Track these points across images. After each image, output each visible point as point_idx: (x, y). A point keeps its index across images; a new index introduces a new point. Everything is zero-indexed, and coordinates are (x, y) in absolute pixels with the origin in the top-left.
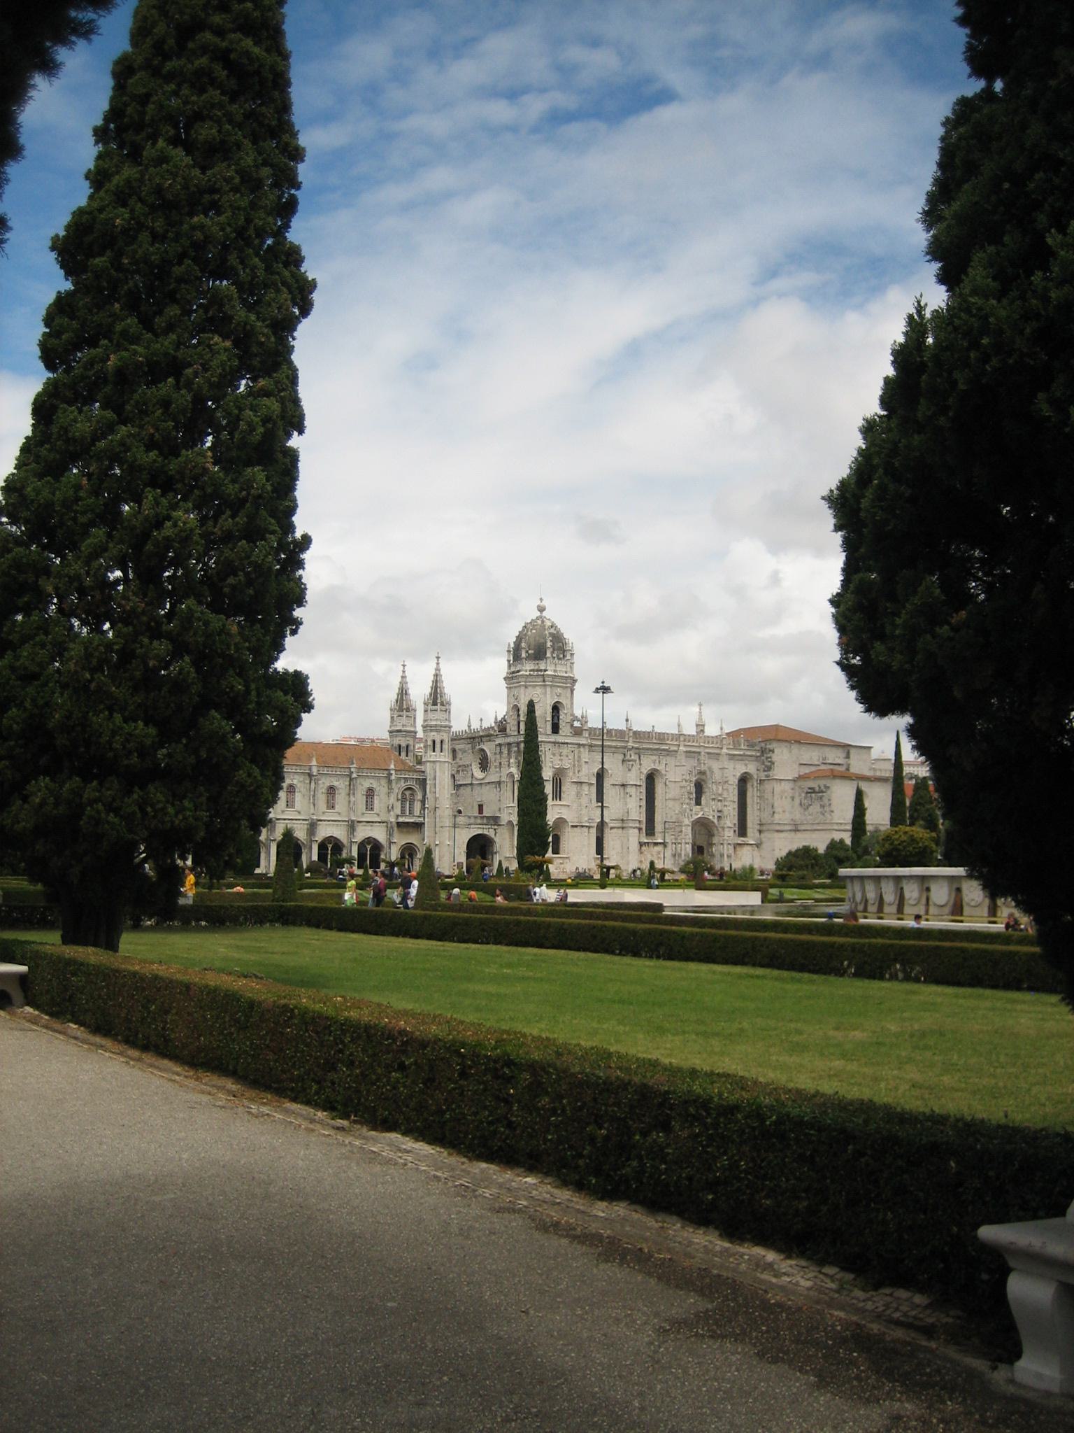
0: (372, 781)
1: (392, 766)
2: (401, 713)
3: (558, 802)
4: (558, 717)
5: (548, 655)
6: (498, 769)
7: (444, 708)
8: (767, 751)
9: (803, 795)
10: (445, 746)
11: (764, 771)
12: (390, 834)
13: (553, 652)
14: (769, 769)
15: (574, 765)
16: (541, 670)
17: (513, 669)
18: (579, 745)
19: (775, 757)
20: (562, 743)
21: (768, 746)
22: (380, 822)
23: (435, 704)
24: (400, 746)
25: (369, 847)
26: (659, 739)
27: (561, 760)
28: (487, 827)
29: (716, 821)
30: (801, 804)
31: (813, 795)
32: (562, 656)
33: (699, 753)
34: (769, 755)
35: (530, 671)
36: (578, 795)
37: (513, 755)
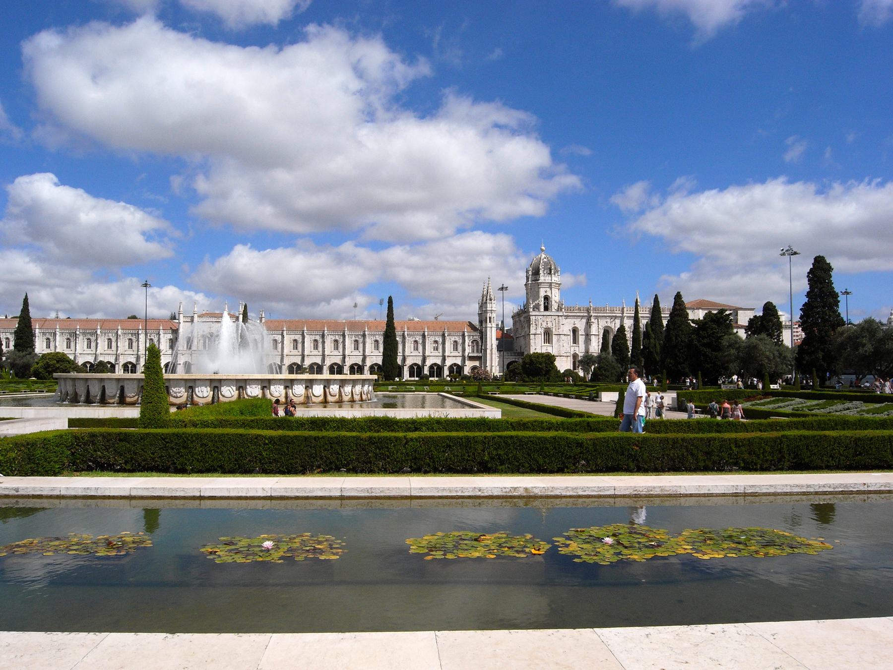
0: (456, 337)
3: (548, 344)
4: (548, 303)
5: (541, 272)
7: (490, 302)
10: (492, 320)
12: (464, 361)
13: (544, 271)
15: (556, 326)
18: (558, 316)
20: (548, 316)
25: (455, 368)
26: (611, 310)
27: (547, 324)
32: (548, 272)
36: (558, 340)
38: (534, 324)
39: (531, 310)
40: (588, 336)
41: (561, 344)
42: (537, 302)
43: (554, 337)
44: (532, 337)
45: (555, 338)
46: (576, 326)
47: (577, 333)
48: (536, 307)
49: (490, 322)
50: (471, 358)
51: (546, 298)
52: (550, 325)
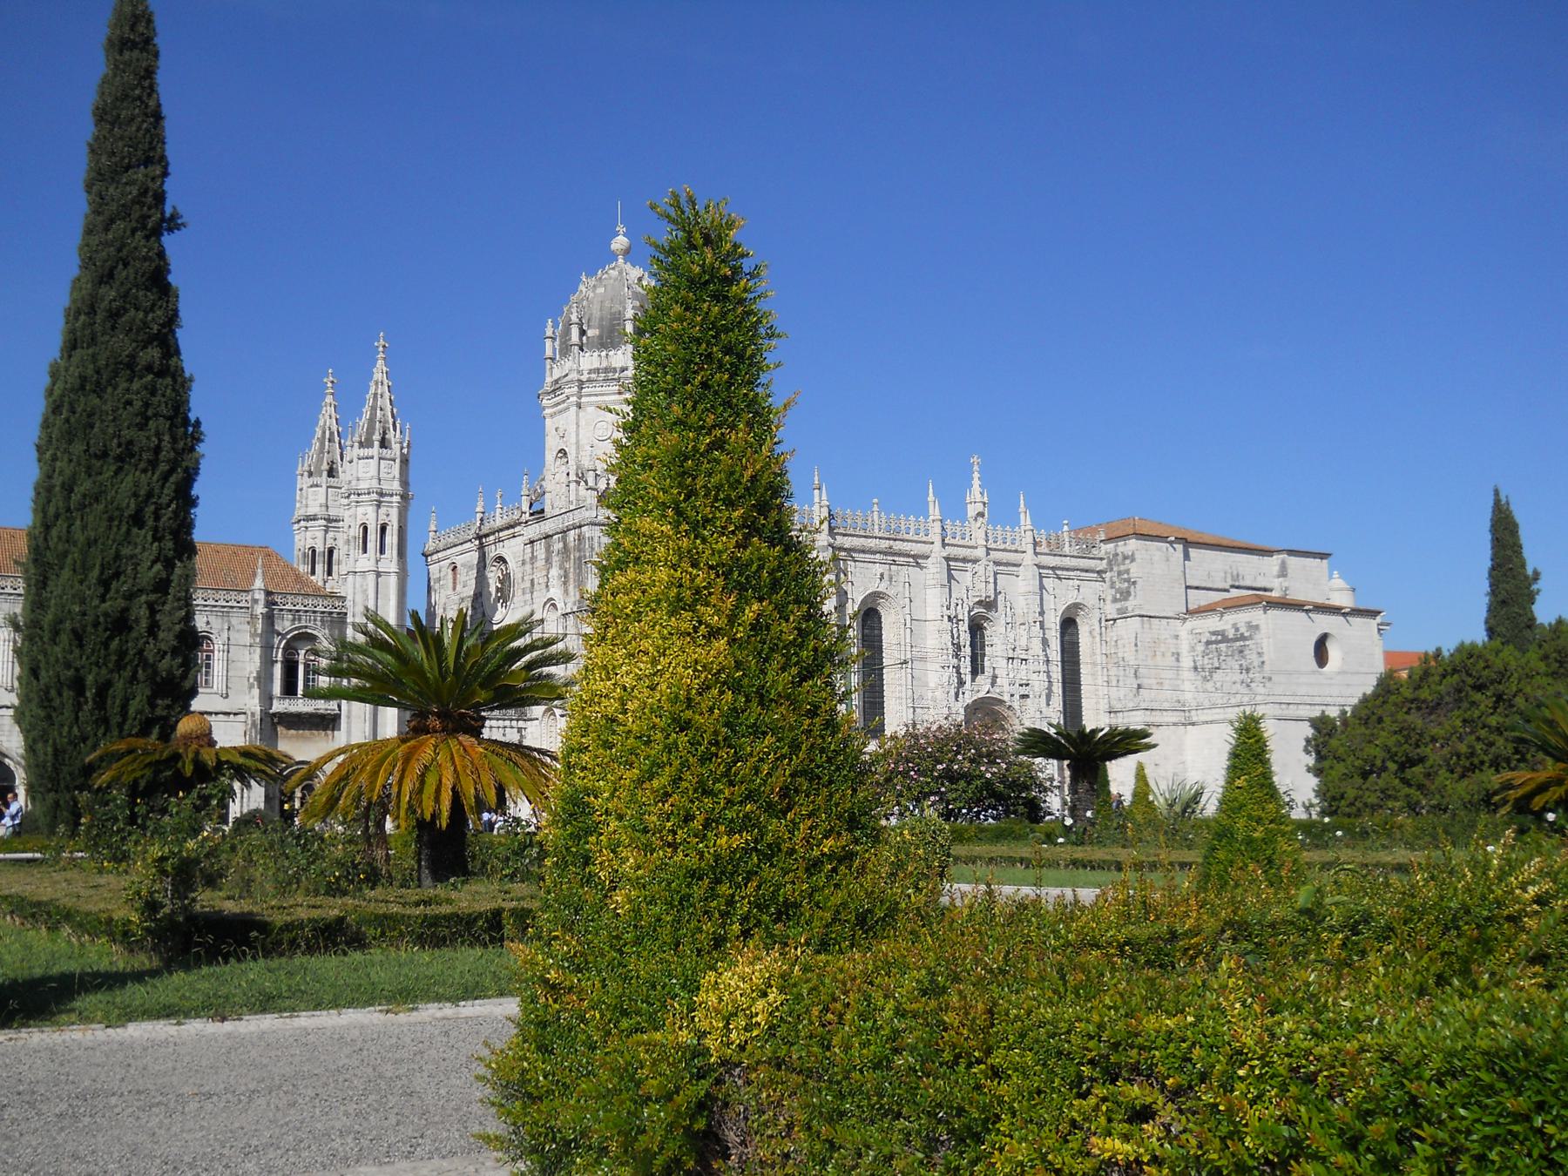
1: (259, 583)
2: (316, 480)
6: (528, 596)
8: (1120, 558)
9: (1200, 648)
11: (1115, 600)
14: (1126, 595)
16: (614, 371)
17: (557, 373)
19: (1135, 570)
21: (1120, 550)
22: (227, 714)
24: (314, 551)
28: (501, 723)
29: (1016, 705)
30: (1196, 668)
31: (1223, 646)
33: (975, 561)
34: (1122, 568)
35: (590, 372)
37: (555, 559)
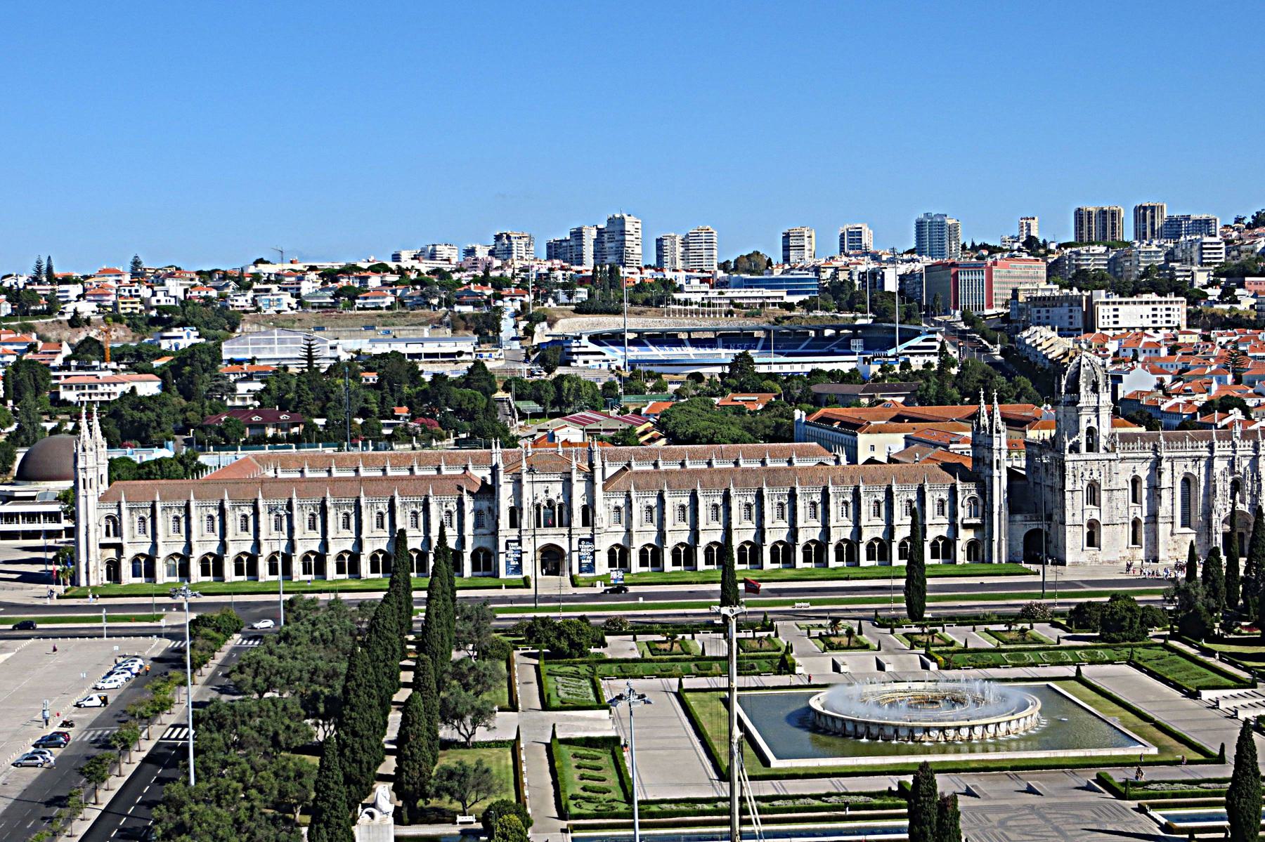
5: (1082, 390)
18: (1110, 460)
23: (991, 432)
36: (1110, 500)
38: (1071, 474)
39: (1067, 452)
40: (1155, 490)
41: (1114, 504)
42: (1075, 439)
43: (1103, 492)
44: (1068, 495)
45: (1104, 496)
46: (1137, 473)
47: (1138, 486)
48: (1075, 448)
49: (998, 468)
50: (966, 527)
51: (1090, 431)
52: (1095, 475)
